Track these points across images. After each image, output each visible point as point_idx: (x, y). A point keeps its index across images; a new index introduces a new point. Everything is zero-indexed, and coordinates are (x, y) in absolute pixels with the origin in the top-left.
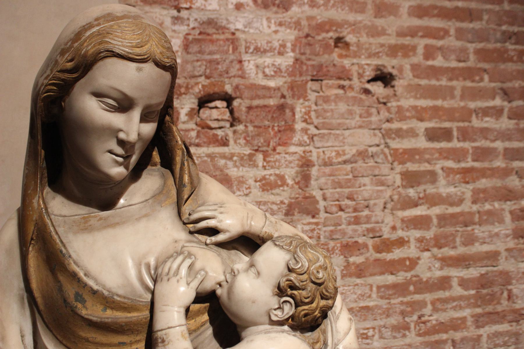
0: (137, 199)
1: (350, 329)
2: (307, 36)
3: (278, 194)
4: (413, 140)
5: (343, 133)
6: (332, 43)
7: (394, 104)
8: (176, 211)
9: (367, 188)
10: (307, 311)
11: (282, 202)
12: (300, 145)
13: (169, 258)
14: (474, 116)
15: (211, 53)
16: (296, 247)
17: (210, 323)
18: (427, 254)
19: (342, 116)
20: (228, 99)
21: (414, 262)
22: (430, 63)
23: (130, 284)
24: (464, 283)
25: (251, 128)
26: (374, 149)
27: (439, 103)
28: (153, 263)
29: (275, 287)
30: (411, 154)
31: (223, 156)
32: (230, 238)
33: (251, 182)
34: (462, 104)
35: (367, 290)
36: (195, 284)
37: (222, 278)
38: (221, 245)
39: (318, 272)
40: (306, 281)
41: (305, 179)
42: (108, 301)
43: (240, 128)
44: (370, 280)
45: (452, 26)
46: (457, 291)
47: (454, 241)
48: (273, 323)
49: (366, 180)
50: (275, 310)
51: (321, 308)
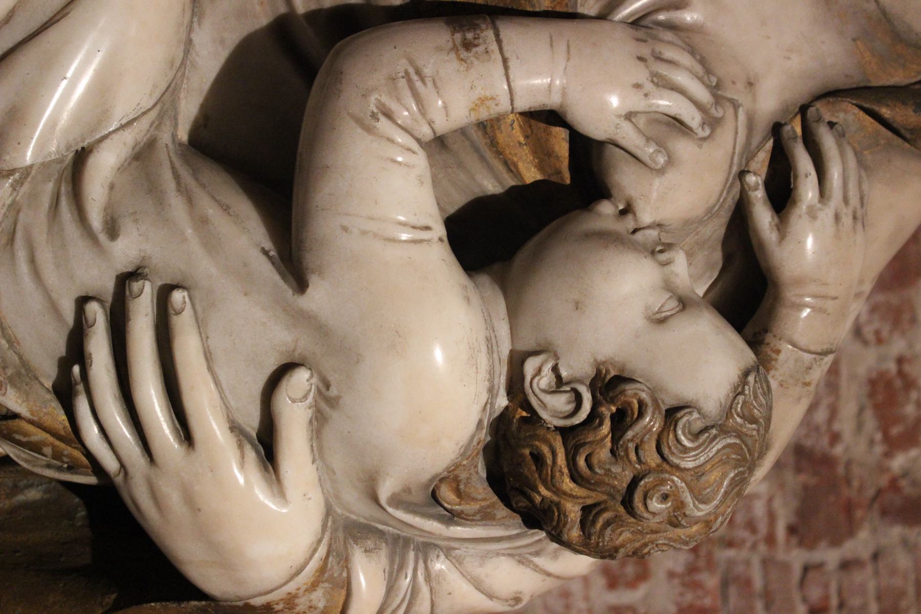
1: (490, 596)
3: (860, 426)
8: (841, 83)
10: (549, 462)
11: (835, 438)
13: (702, 62)
16: (739, 435)
17: (513, 189)
28: (689, 17)
29: (622, 370)
32: (761, 245)
33: (898, 346)
36: (629, 136)
37: (646, 216)
39: (665, 497)
40: (640, 461)
48: (517, 362)
50: (555, 369)
51: (558, 505)
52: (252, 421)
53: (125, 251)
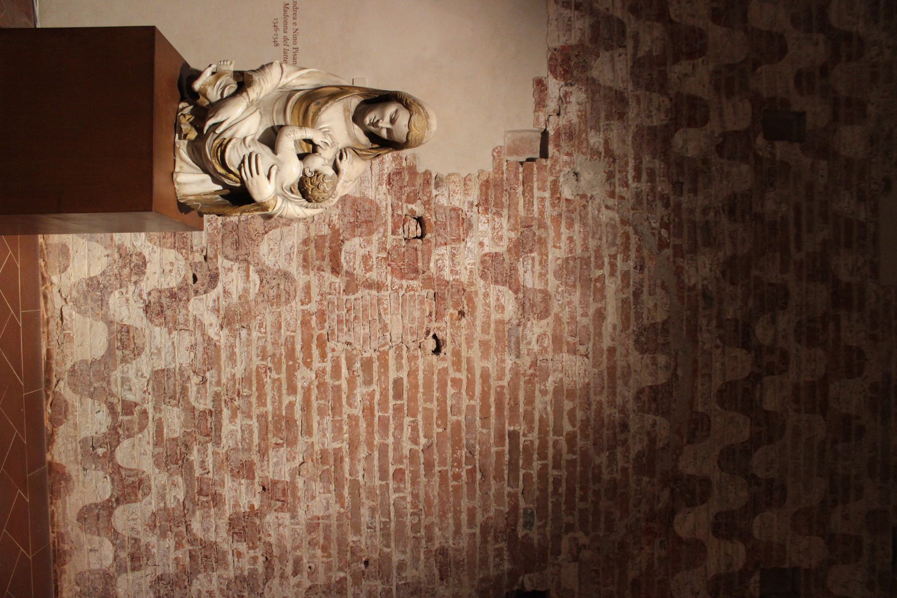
0: (356, 132)
2: (464, 290)
4: (394, 368)
5: (400, 314)
6: (460, 308)
7: (420, 353)
9: (362, 331)
11: (355, 269)
12: (392, 283)
14: (412, 419)
15: (450, 224)
18: (314, 376)
19: (411, 314)
20: (421, 237)
21: (308, 365)
22: (449, 383)
23: (321, 124)
24: (291, 405)
25: (403, 250)
26: (388, 337)
27: (421, 390)
30: (384, 365)
31: (385, 231)
33: (368, 249)
34: (420, 409)
35: (292, 328)
36: (321, 144)
38: (335, 162)
41: (369, 285)
42: (316, 114)
43: (404, 243)
44: (299, 331)
45: (477, 402)
46: (286, 400)
47: (321, 399)
48: (304, 170)
49: (367, 330)
52: (267, 173)
53: (251, 150)
